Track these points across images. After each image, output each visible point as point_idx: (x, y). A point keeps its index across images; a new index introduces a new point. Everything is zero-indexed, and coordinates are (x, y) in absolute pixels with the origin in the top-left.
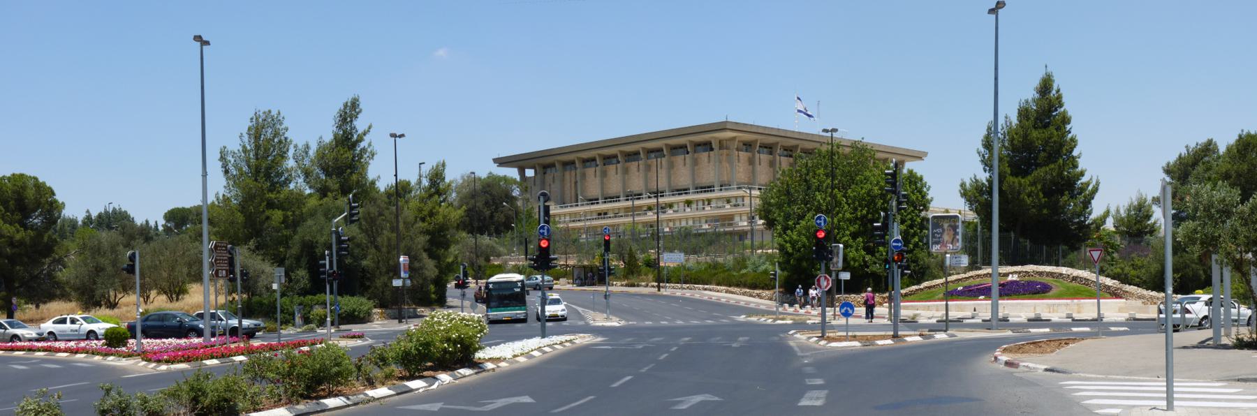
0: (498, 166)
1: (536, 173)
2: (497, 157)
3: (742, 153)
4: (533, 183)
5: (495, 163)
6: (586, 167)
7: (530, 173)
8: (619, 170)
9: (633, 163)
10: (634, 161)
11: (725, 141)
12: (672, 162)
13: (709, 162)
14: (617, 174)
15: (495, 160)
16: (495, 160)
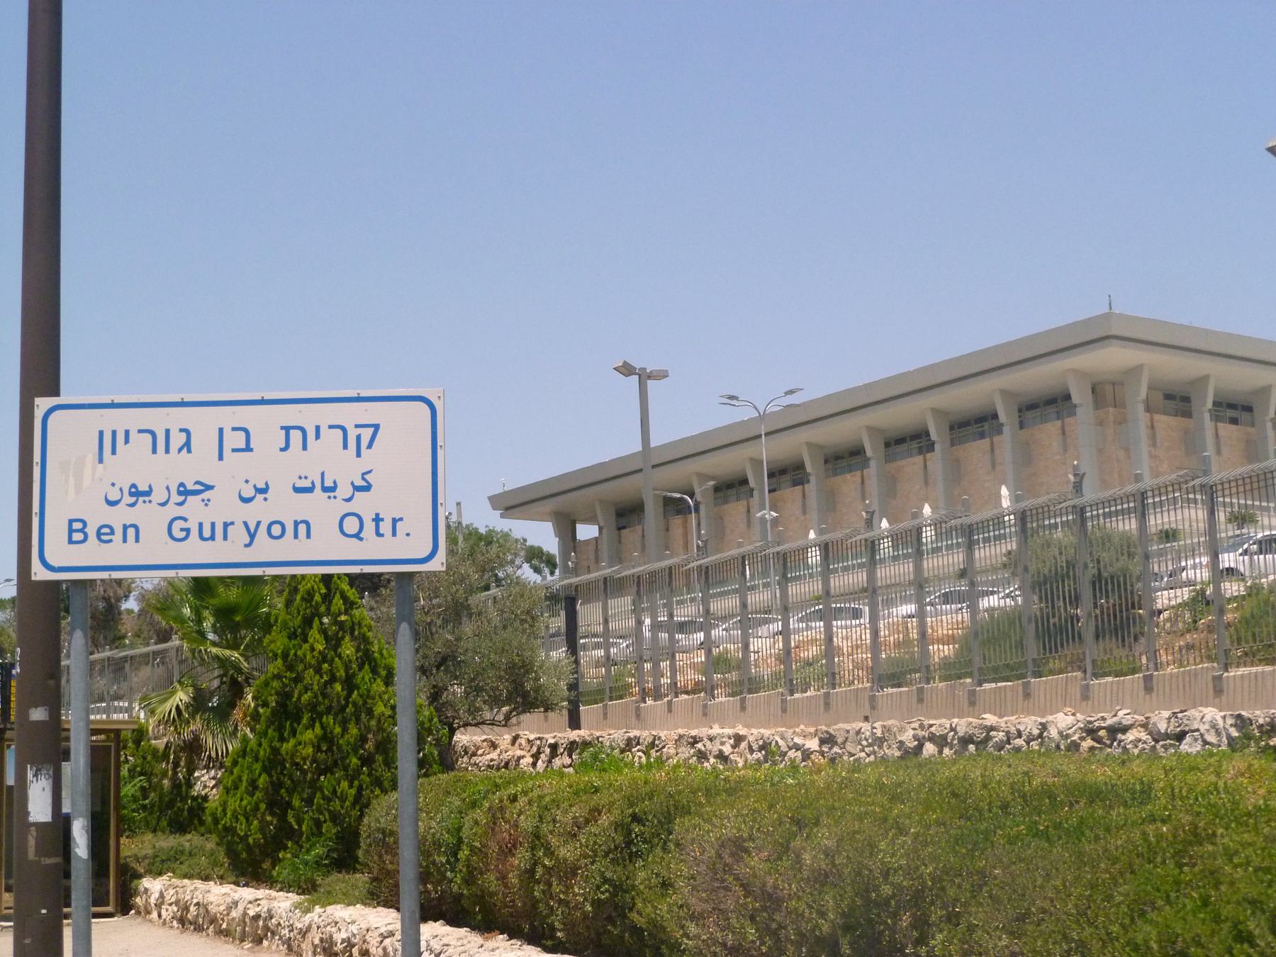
0: (502, 516)
1: (601, 529)
2: (499, 490)
3: (1164, 418)
4: (592, 556)
5: (494, 508)
6: (726, 502)
7: (586, 532)
8: (813, 501)
9: (848, 476)
10: (850, 469)
11: (1109, 388)
12: (958, 461)
13: (1065, 450)
14: (804, 512)
15: (495, 501)
16: (495, 501)
